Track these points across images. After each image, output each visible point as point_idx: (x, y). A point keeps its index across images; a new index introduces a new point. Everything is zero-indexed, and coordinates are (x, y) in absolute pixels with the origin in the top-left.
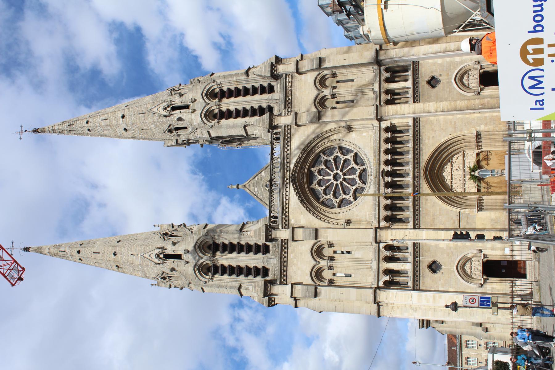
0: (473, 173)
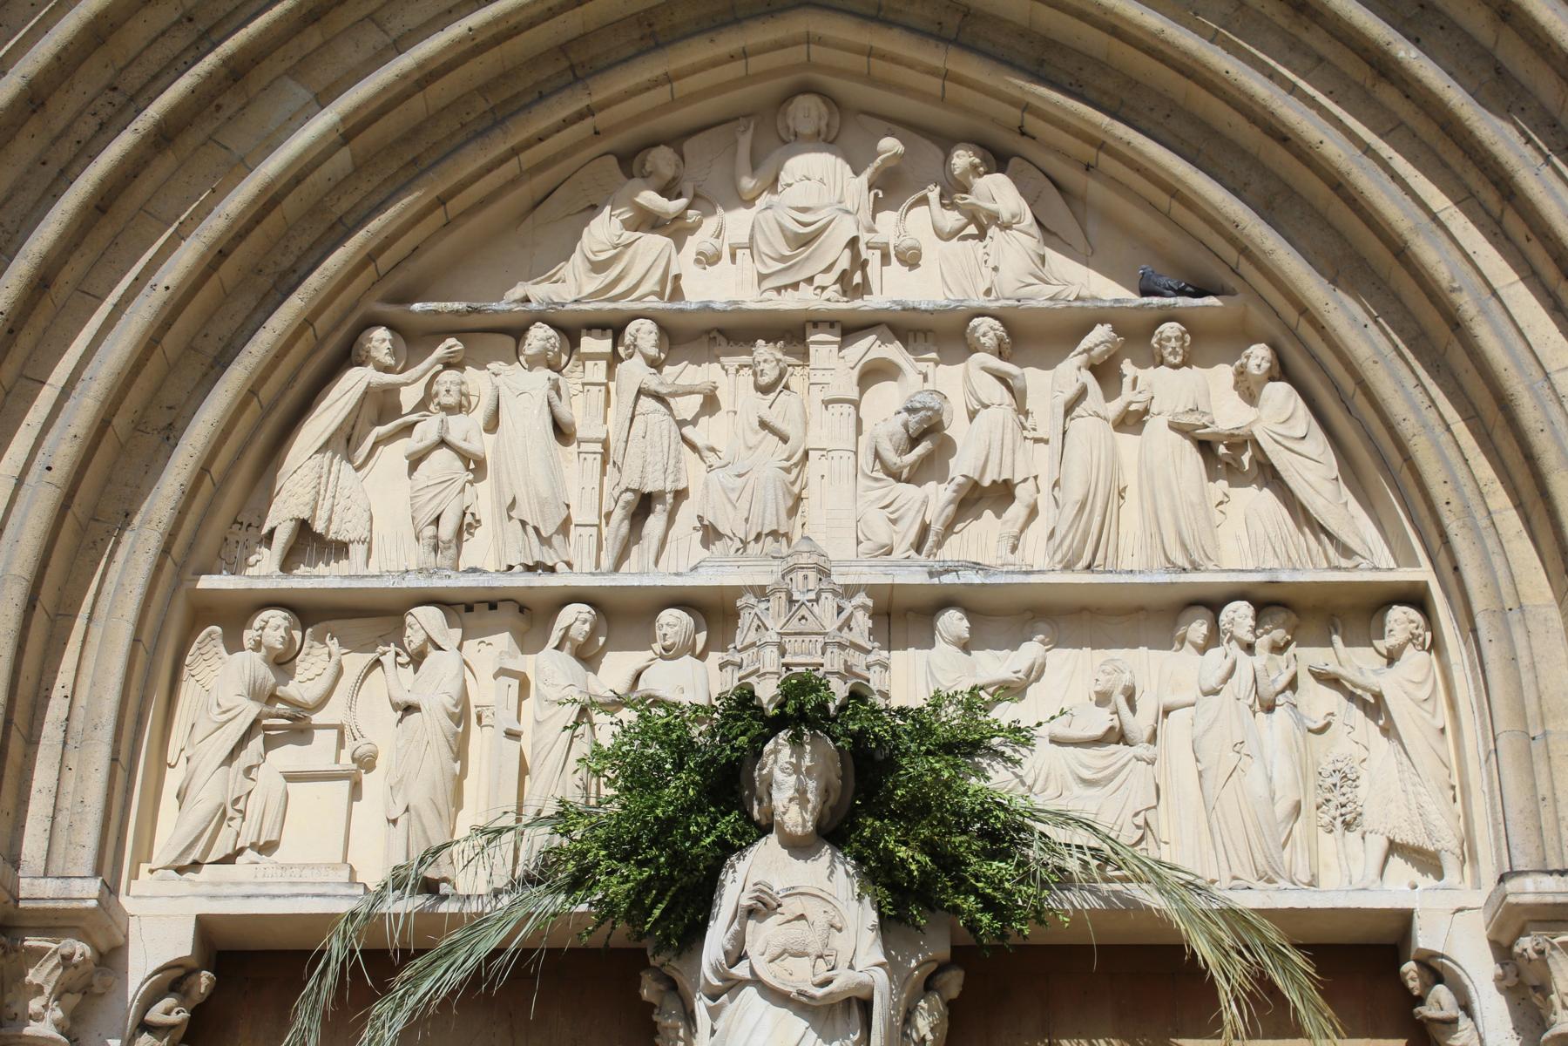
0: (789, 779)
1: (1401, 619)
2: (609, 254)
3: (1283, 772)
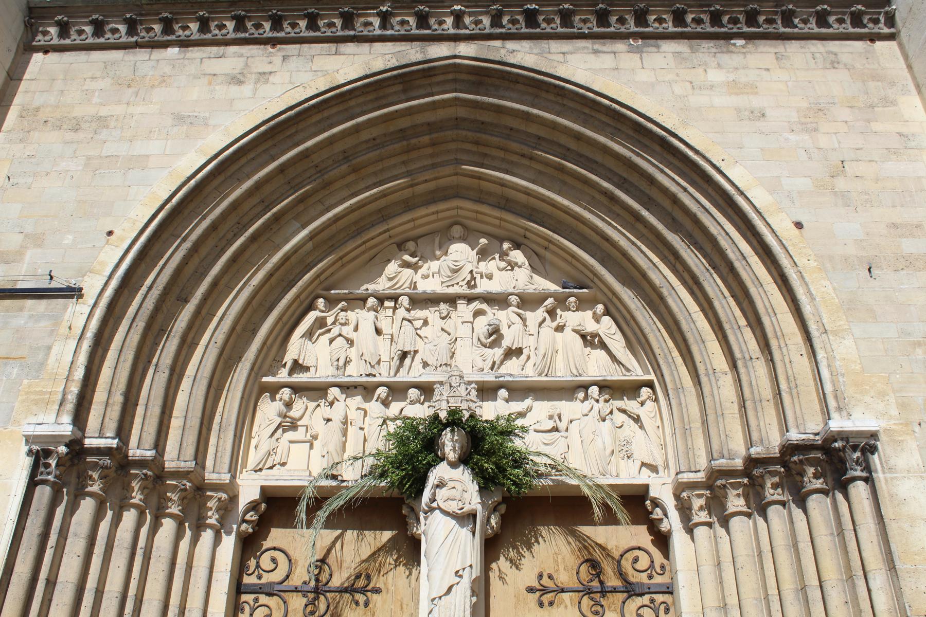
0: (450, 443)
1: (645, 392)
2: (394, 275)
3: (608, 440)
